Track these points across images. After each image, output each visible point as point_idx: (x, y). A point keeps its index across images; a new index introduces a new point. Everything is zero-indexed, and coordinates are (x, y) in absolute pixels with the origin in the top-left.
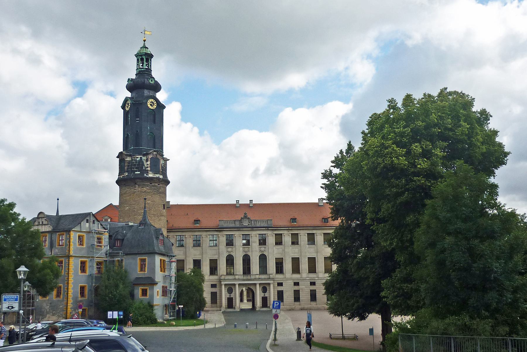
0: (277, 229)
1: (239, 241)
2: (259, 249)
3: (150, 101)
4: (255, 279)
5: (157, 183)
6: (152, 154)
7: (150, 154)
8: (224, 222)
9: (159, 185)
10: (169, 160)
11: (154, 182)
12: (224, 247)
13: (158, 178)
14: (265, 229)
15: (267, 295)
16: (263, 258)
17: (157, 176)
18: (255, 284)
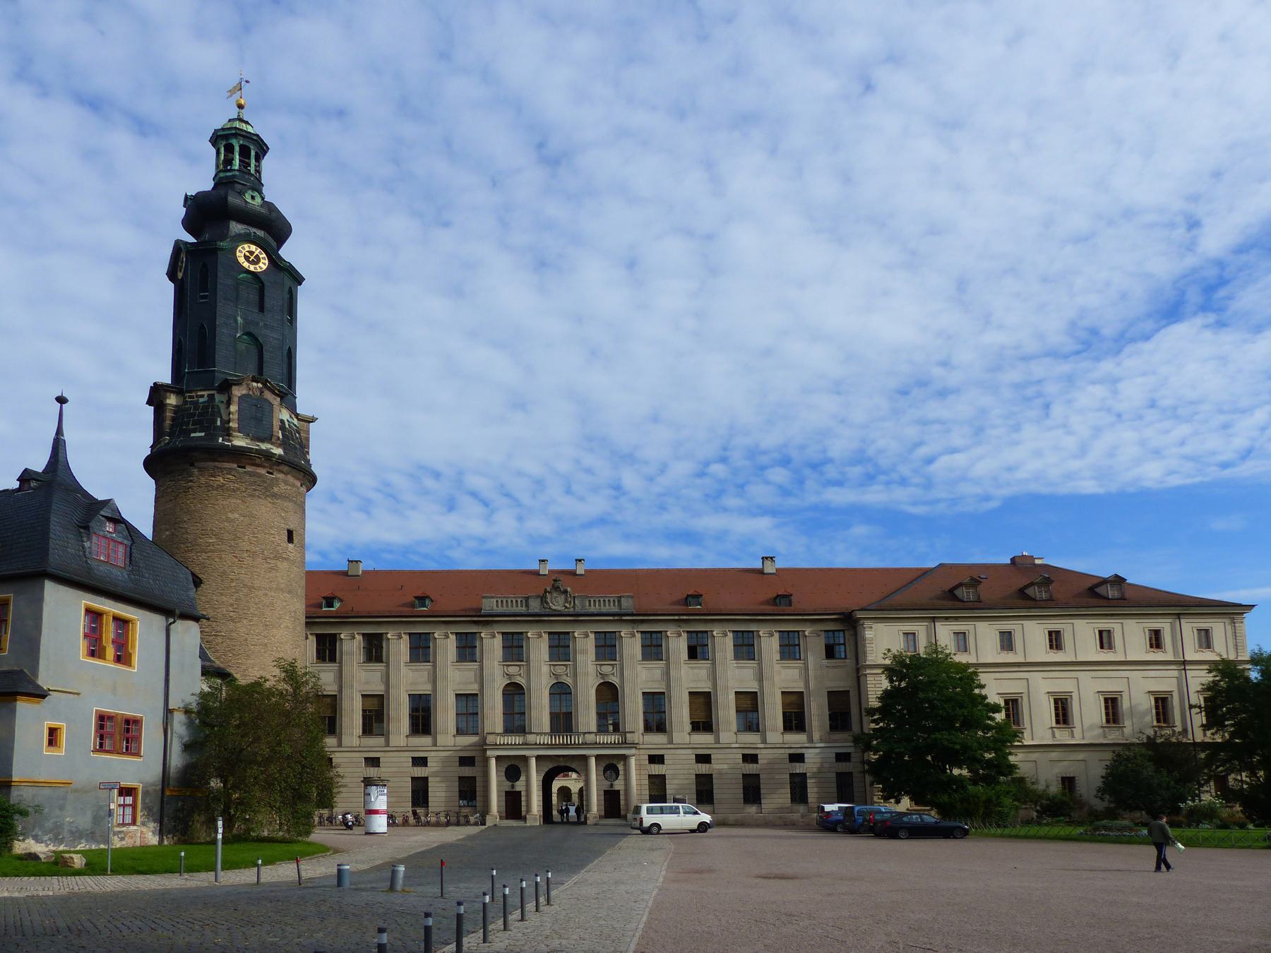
0: (646, 618)
1: (539, 647)
2: (597, 670)
3: (243, 248)
4: (585, 745)
5: (264, 467)
6: (245, 386)
7: (238, 383)
8: (497, 601)
9: (268, 472)
10: (313, 420)
11: (251, 462)
12: (496, 663)
13: (268, 455)
14: (611, 618)
15: (619, 785)
16: (609, 694)
17: (264, 446)
18: (585, 759)
